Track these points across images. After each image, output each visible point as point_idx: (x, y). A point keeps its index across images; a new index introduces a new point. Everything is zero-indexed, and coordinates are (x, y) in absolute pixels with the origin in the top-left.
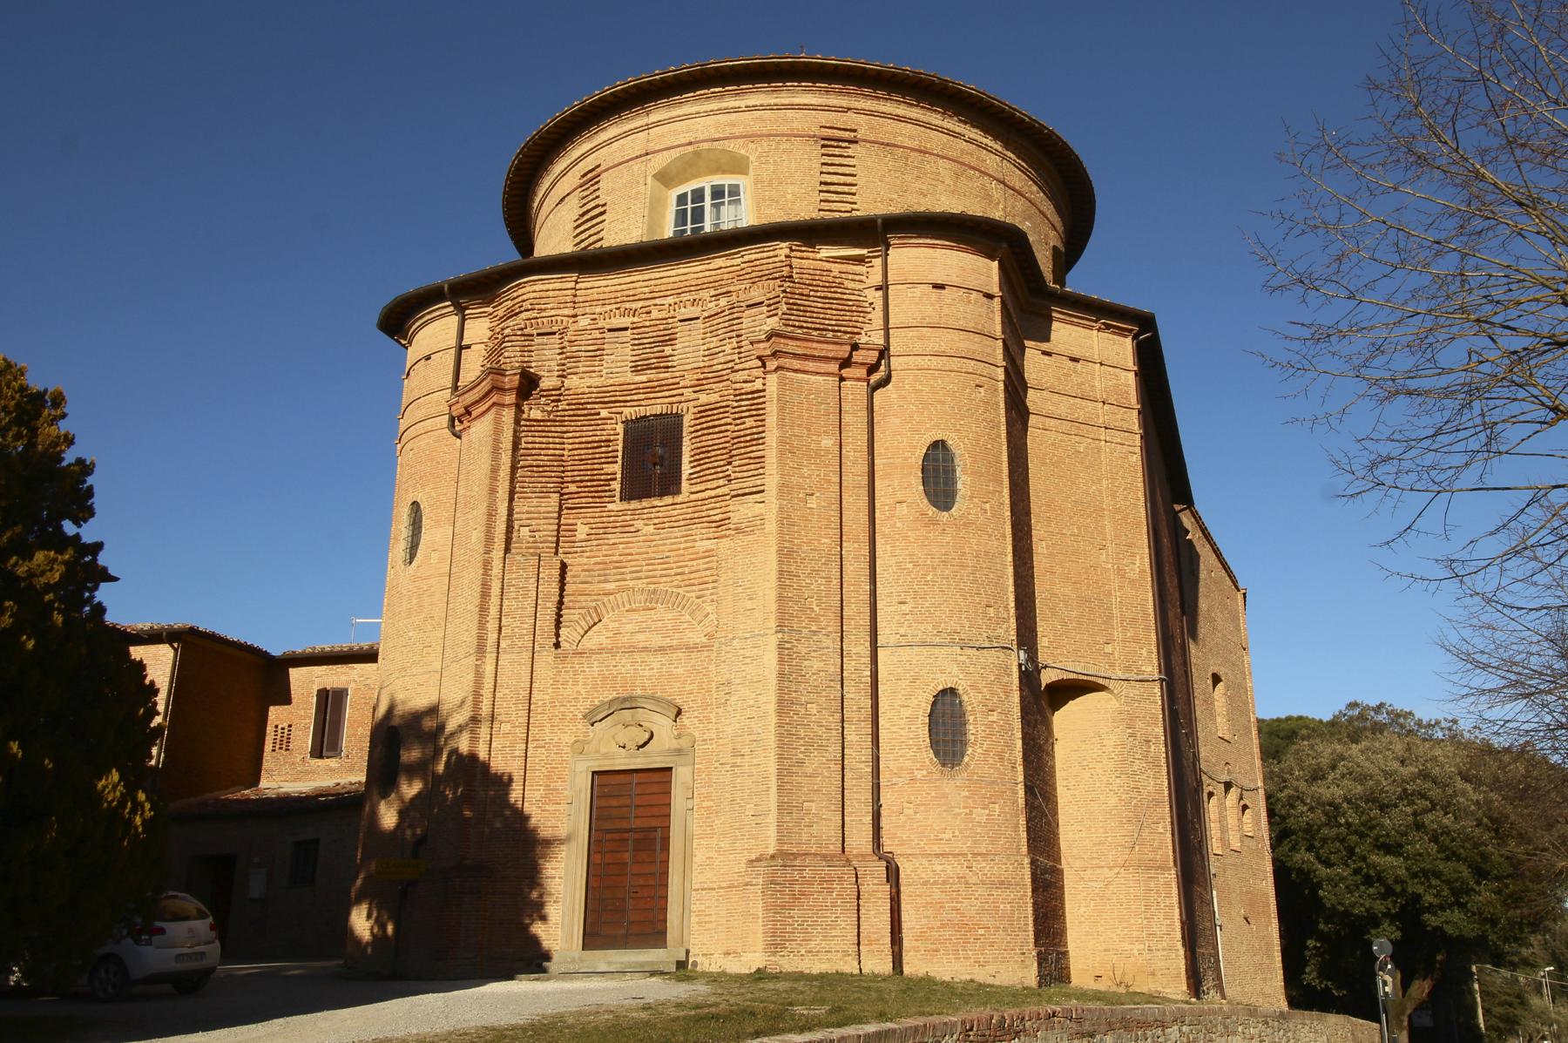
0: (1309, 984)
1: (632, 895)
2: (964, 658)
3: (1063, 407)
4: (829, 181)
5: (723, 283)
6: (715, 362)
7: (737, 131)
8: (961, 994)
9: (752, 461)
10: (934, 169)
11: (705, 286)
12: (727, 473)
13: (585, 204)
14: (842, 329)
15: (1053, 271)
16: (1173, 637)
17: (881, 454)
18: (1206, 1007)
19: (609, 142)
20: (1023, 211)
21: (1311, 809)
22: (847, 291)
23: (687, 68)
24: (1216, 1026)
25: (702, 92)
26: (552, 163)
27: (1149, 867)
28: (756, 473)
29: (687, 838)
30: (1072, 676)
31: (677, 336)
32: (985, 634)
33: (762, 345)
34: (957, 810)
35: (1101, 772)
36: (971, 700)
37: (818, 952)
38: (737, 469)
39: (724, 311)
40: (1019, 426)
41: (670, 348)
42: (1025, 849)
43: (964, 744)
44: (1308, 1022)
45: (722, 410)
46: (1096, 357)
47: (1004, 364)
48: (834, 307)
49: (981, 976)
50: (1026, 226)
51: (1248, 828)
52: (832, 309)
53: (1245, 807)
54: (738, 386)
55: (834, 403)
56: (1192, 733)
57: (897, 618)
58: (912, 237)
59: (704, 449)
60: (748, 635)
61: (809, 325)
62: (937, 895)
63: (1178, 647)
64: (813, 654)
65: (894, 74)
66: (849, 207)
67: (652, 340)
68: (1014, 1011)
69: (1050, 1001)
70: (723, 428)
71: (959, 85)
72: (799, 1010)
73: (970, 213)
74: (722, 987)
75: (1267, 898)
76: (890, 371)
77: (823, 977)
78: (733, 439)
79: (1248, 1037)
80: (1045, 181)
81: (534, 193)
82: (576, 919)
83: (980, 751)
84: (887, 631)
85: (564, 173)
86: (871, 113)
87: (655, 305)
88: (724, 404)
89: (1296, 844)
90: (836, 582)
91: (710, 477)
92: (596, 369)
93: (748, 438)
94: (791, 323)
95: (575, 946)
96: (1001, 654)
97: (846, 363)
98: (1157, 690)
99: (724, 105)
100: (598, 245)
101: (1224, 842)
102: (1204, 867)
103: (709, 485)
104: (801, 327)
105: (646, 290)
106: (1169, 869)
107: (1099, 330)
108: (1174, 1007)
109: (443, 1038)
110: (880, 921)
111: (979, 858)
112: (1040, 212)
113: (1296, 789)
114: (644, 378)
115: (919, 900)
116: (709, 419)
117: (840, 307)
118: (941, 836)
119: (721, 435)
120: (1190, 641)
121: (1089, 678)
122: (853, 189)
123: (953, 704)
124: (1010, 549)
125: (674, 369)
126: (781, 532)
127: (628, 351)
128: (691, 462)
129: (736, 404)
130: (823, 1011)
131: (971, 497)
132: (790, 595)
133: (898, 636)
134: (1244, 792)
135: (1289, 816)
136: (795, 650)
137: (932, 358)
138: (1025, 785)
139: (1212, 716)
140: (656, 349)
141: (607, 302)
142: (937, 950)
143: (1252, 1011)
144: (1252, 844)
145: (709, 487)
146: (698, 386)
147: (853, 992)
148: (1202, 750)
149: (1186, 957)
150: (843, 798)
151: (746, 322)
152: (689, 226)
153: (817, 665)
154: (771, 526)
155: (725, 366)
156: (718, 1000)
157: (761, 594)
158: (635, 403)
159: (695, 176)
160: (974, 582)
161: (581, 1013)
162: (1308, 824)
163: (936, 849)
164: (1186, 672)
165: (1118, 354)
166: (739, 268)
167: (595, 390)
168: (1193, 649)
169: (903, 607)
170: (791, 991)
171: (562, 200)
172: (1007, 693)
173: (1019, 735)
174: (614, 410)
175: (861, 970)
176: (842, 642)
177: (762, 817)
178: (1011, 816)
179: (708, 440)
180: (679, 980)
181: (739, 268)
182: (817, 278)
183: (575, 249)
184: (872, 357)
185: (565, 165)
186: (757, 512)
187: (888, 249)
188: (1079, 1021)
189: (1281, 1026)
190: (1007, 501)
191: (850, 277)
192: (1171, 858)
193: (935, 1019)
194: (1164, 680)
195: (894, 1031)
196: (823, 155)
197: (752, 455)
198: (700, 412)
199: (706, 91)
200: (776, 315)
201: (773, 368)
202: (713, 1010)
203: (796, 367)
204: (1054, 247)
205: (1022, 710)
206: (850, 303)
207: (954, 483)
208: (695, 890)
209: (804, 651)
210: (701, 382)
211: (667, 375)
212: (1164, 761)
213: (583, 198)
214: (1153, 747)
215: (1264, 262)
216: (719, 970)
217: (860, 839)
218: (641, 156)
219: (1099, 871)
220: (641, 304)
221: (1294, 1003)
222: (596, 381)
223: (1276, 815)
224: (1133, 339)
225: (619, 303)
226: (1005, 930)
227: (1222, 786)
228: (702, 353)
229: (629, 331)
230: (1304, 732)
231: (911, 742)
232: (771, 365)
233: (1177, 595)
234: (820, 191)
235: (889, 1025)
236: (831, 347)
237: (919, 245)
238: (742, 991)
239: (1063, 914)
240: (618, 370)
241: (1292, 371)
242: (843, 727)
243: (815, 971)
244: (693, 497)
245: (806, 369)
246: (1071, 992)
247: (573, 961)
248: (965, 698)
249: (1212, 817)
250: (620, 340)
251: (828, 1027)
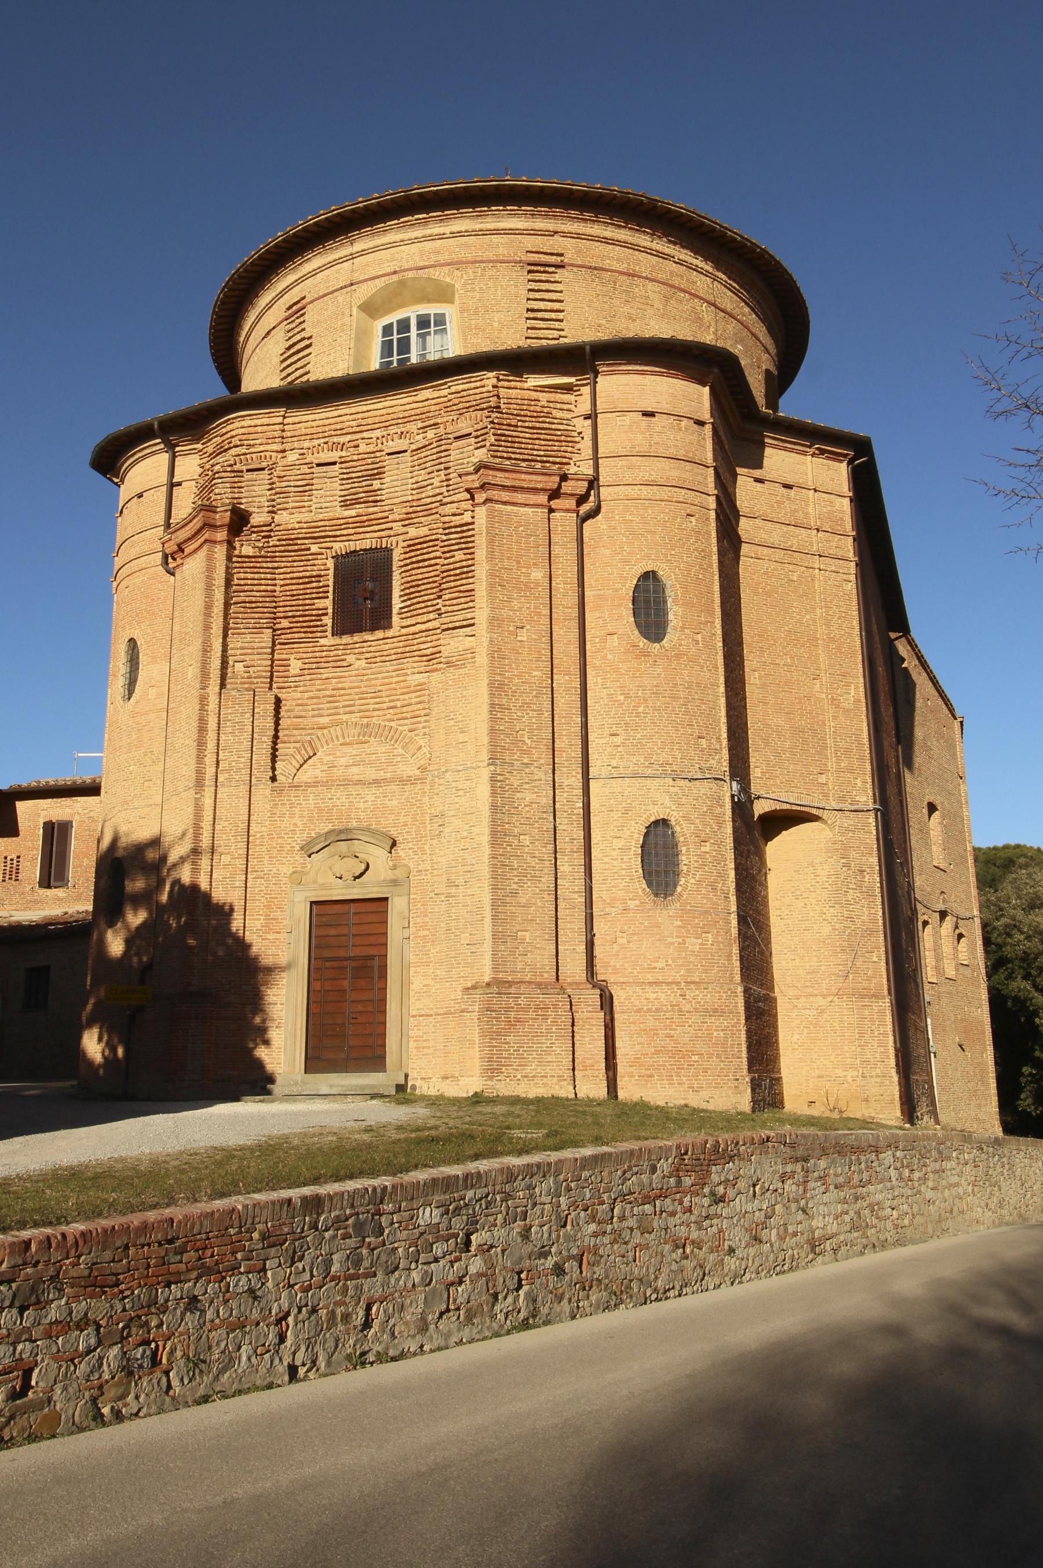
0: (1024, 1111)
1: (353, 1021)
2: (676, 789)
3: (776, 535)
4: (536, 307)
5: (430, 414)
6: (424, 495)
7: (442, 259)
8: (676, 1119)
9: (462, 595)
10: (643, 293)
11: (412, 419)
12: (437, 607)
13: (291, 338)
14: (551, 459)
15: (766, 396)
16: (888, 767)
17: (591, 586)
18: (920, 1133)
19: (314, 273)
20: (735, 334)
21: (1028, 938)
22: (556, 421)
23: (390, 194)
24: (930, 1151)
25: (406, 219)
26: (257, 296)
27: (863, 995)
28: (466, 606)
29: (404, 967)
30: (788, 807)
31: (386, 469)
32: (698, 766)
33: (470, 478)
34: (670, 940)
35: (814, 901)
36: (683, 831)
37: (534, 1076)
38: (447, 603)
39: (432, 444)
40: (731, 555)
41: (378, 482)
42: (738, 978)
43: (677, 874)
44: (1023, 1148)
45: (431, 544)
46: (810, 483)
47: (716, 492)
48: (542, 437)
49: (695, 1101)
50: (737, 350)
51: (964, 957)
52: (539, 439)
53: (960, 936)
54: (446, 519)
55: (543, 535)
56: (908, 864)
57: (609, 749)
58: (620, 364)
59: (414, 583)
60: (461, 768)
61: (518, 456)
62: (651, 1022)
63: (893, 776)
64: (526, 786)
65: (601, 195)
66: (556, 334)
67: (360, 474)
68: (728, 1136)
69: (763, 1125)
70: (433, 562)
71: (668, 204)
72: (517, 1133)
73: (680, 337)
74: (441, 1110)
75: (982, 1026)
76: (600, 502)
77: (539, 1101)
78: (442, 572)
79: (963, 1162)
80: (758, 302)
81: (240, 327)
82: (298, 1044)
83: (692, 881)
84: (599, 763)
85: (269, 306)
86: (578, 236)
87: (362, 439)
88: (433, 537)
89: (1013, 972)
90: (547, 714)
91: (420, 611)
92: (306, 504)
93: (458, 571)
94: (499, 454)
95: (297, 1070)
96: (713, 785)
97: (555, 494)
98: (872, 820)
99: (428, 232)
100: (305, 379)
101: (939, 970)
102: (919, 996)
103: (419, 619)
104: (509, 458)
105: (354, 423)
106: (883, 997)
107: (813, 455)
108: (888, 1132)
109: (175, 1157)
110: (595, 1047)
111: (692, 986)
112: (753, 334)
113: (1013, 918)
114: (353, 513)
115: (633, 1027)
116: (418, 552)
117: (549, 437)
118: (654, 965)
119: (431, 569)
120: (906, 770)
121: (802, 809)
122: (561, 316)
123: (665, 835)
124: (722, 680)
125: (383, 503)
126: (492, 665)
127: (336, 485)
128: (401, 596)
129: (445, 538)
130: (540, 1135)
131: (683, 628)
132: (502, 728)
133: (610, 768)
134: (959, 921)
135: (1005, 944)
136: (507, 782)
137: (643, 487)
138: (738, 915)
139: (928, 846)
140: (364, 484)
141: (315, 436)
142: (652, 1076)
143: (966, 1137)
144: (967, 972)
145: (419, 621)
146: (407, 520)
147: (569, 1116)
148: (917, 879)
149: (900, 1084)
150: (557, 928)
151: (454, 455)
152: (395, 358)
153: (529, 797)
154: (482, 659)
155: (434, 499)
156: (438, 1123)
157: (473, 727)
158: (344, 538)
159: (400, 306)
160: (686, 713)
161: (305, 1135)
162: (1024, 952)
163: (650, 978)
164: (901, 801)
165: (832, 480)
166: (445, 399)
167: (305, 525)
168: (908, 778)
169: (615, 739)
170: (509, 1114)
171: (268, 333)
172: (720, 824)
173: (732, 865)
174: (324, 545)
175: (576, 1094)
176: (554, 773)
177: (477, 946)
178: (725, 946)
179: (418, 574)
180: (399, 1102)
181: (445, 399)
182: (525, 407)
183: (282, 383)
184: (582, 487)
185: (270, 298)
186: (467, 645)
187: (596, 377)
188: (793, 1146)
189: (996, 1152)
190: (719, 632)
191: (559, 406)
192: (886, 987)
193: (651, 1144)
194: (878, 810)
195: (610, 1154)
196: (529, 281)
197: (462, 588)
198: (409, 546)
199: (410, 218)
200: (484, 446)
201: (482, 501)
202: (433, 1133)
203: (504, 500)
204: (767, 371)
205: (735, 840)
206: (559, 433)
207: (665, 614)
208: (414, 1016)
209: (516, 783)
210: (410, 516)
211: (376, 509)
212: (878, 890)
213: (288, 332)
214: (867, 877)
215: (988, 387)
216: (438, 1094)
217: (574, 967)
218: (346, 287)
219: (812, 999)
220: (349, 437)
221: (1009, 1129)
222: (305, 516)
223: (993, 944)
224: (848, 464)
225: (326, 436)
226: (718, 1056)
227: (937, 915)
228: (410, 486)
229: (338, 465)
230: (1022, 860)
231: (624, 872)
232: (480, 497)
233: (892, 724)
234: (527, 319)
235: (605, 1149)
236: (539, 478)
237: (628, 372)
238: (460, 1114)
239: (777, 1041)
240: (328, 505)
241: (1017, 499)
242: (556, 858)
243: (531, 1095)
244: (404, 631)
245: (515, 500)
246: (784, 1117)
247: (296, 1084)
248: (677, 829)
249: (927, 946)
250: (329, 475)
251: (545, 1150)
